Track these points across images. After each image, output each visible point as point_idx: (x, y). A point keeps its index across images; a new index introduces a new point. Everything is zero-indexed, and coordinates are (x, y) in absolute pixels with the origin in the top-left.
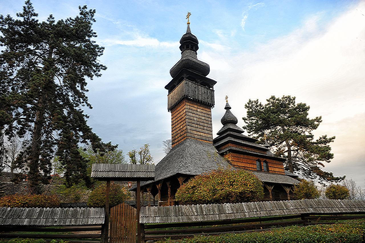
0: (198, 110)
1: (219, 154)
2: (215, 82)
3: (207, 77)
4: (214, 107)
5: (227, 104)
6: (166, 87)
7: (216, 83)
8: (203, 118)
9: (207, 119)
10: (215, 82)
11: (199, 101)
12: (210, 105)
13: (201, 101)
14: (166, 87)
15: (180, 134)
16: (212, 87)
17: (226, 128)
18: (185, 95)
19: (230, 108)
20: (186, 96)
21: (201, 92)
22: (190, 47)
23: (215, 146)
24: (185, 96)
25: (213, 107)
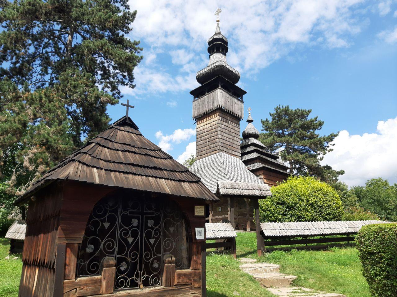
1: (251, 171)
2: (244, 93)
3: (236, 85)
10: (244, 93)
11: (231, 112)
13: (233, 113)
16: (242, 98)
20: (220, 107)
22: (221, 51)
23: (243, 160)
24: (219, 106)
25: (241, 119)
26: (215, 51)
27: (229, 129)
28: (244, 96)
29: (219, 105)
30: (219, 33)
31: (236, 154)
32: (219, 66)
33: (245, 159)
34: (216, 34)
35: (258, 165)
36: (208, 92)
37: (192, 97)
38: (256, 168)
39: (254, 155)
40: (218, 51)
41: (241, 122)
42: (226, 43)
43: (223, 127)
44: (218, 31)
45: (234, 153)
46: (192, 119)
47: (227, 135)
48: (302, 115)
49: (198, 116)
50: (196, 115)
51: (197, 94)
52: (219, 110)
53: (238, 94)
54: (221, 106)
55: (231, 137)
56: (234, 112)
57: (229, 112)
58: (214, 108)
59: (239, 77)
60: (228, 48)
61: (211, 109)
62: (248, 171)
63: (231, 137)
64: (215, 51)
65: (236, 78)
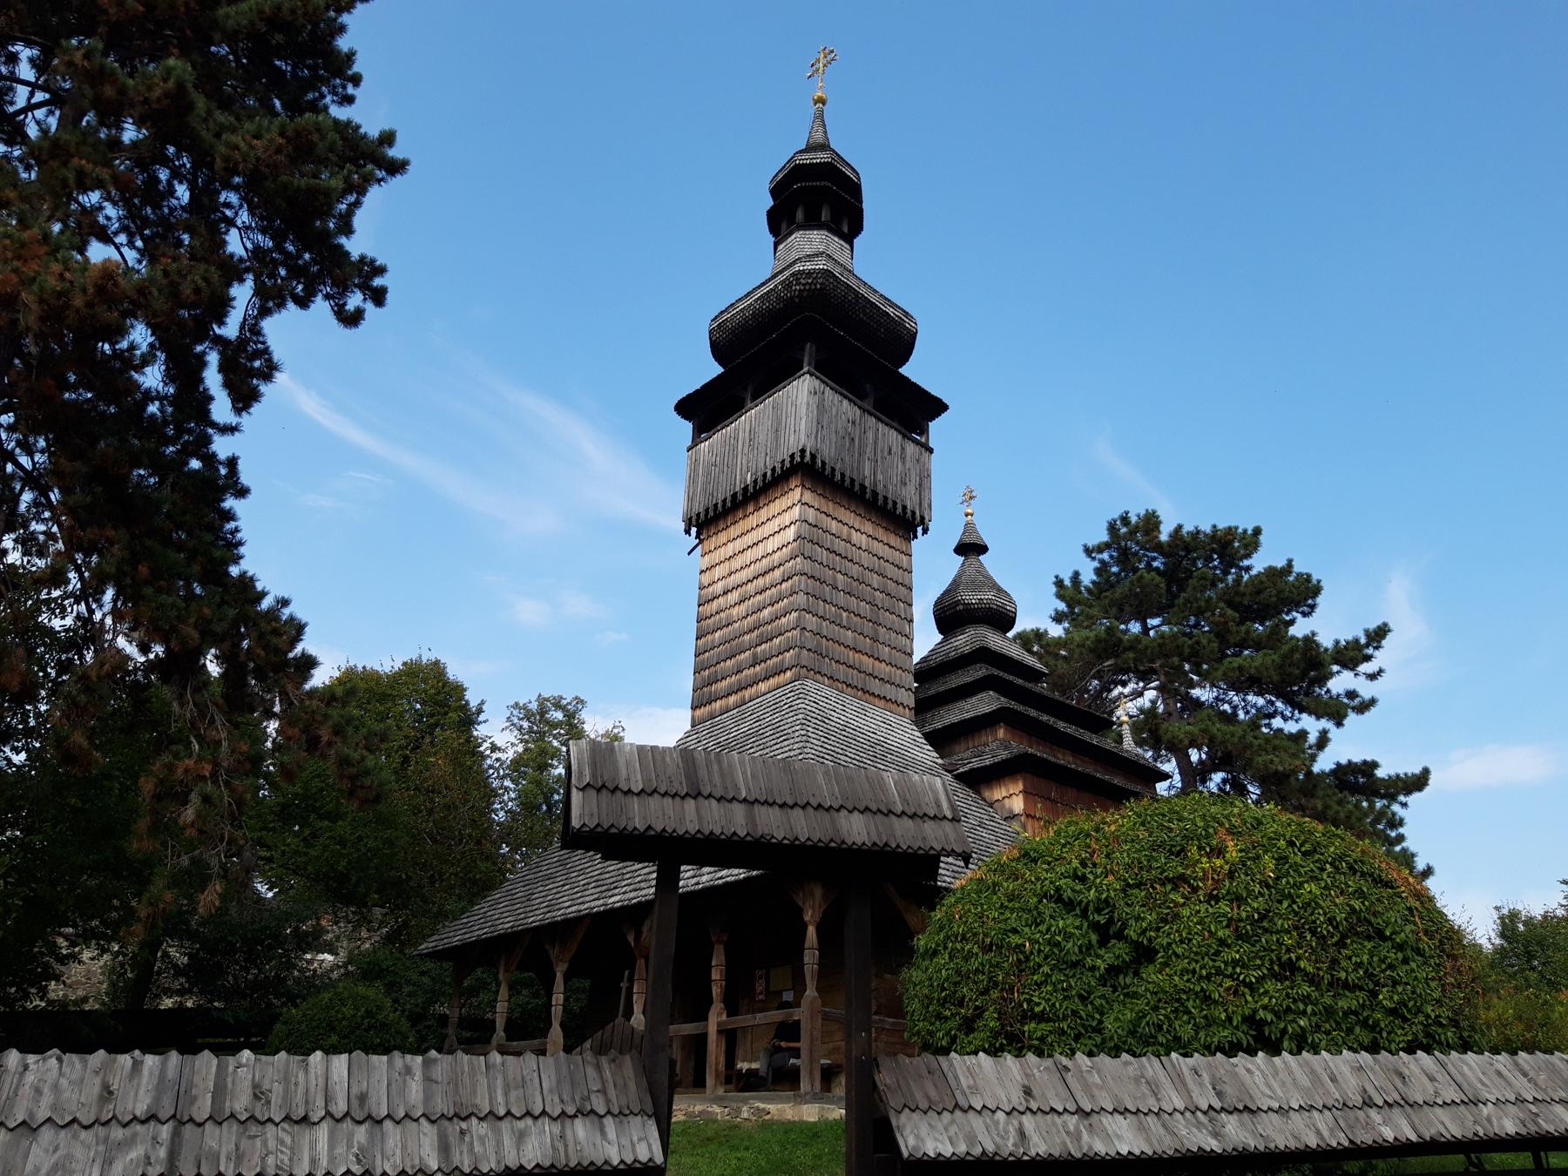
0: (855, 537)
2: (938, 407)
4: (925, 531)
5: (969, 528)
6: (685, 408)
7: (938, 415)
8: (875, 580)
9: (891, 586)
10: (938, 407)
11: (863, 487)
12: (906, 523)
14: (685, 408)
15: (755, 655)
17: (964, 641)
18: (803, 451)
19: (983, 549)
20: (808, 458)
21: (876, 449)
23: (928, 729)
25: (920, 529)
26: (800, 215)
27: (855, 570)
28: (934, 426)
29: (803, 451)
30: (824, 147)
31: (889, 691)
32: (809, 273)
33: (939, 725)
34: (810, 148)
35: (998, 746)
36: (754, 398)
37: (687, 427)
38: (988, 763)
39: (984, 703)
40: (812, 223)
41: (919, 545)
42: (854, 189)
43: (823, 555)
44: (818, 137)
45: (875, 686)
46: (682, 526)
47: (841, 598)
48: (1229, 546)
49: (707, 510)
50: (698, 507)
51: (705, 410)
52: (805, 469)
53: (915, 411)
54: (813, 456)
55: (865, 608)
56: (880, 488)
57: (857, 488)
58: (778, 466)
59: (913, 336)
60: (861, 211)
61: (765, 475)
62: (949, 777)
63: (865, 608)
64: (800, 215)
65: (901, 340)
